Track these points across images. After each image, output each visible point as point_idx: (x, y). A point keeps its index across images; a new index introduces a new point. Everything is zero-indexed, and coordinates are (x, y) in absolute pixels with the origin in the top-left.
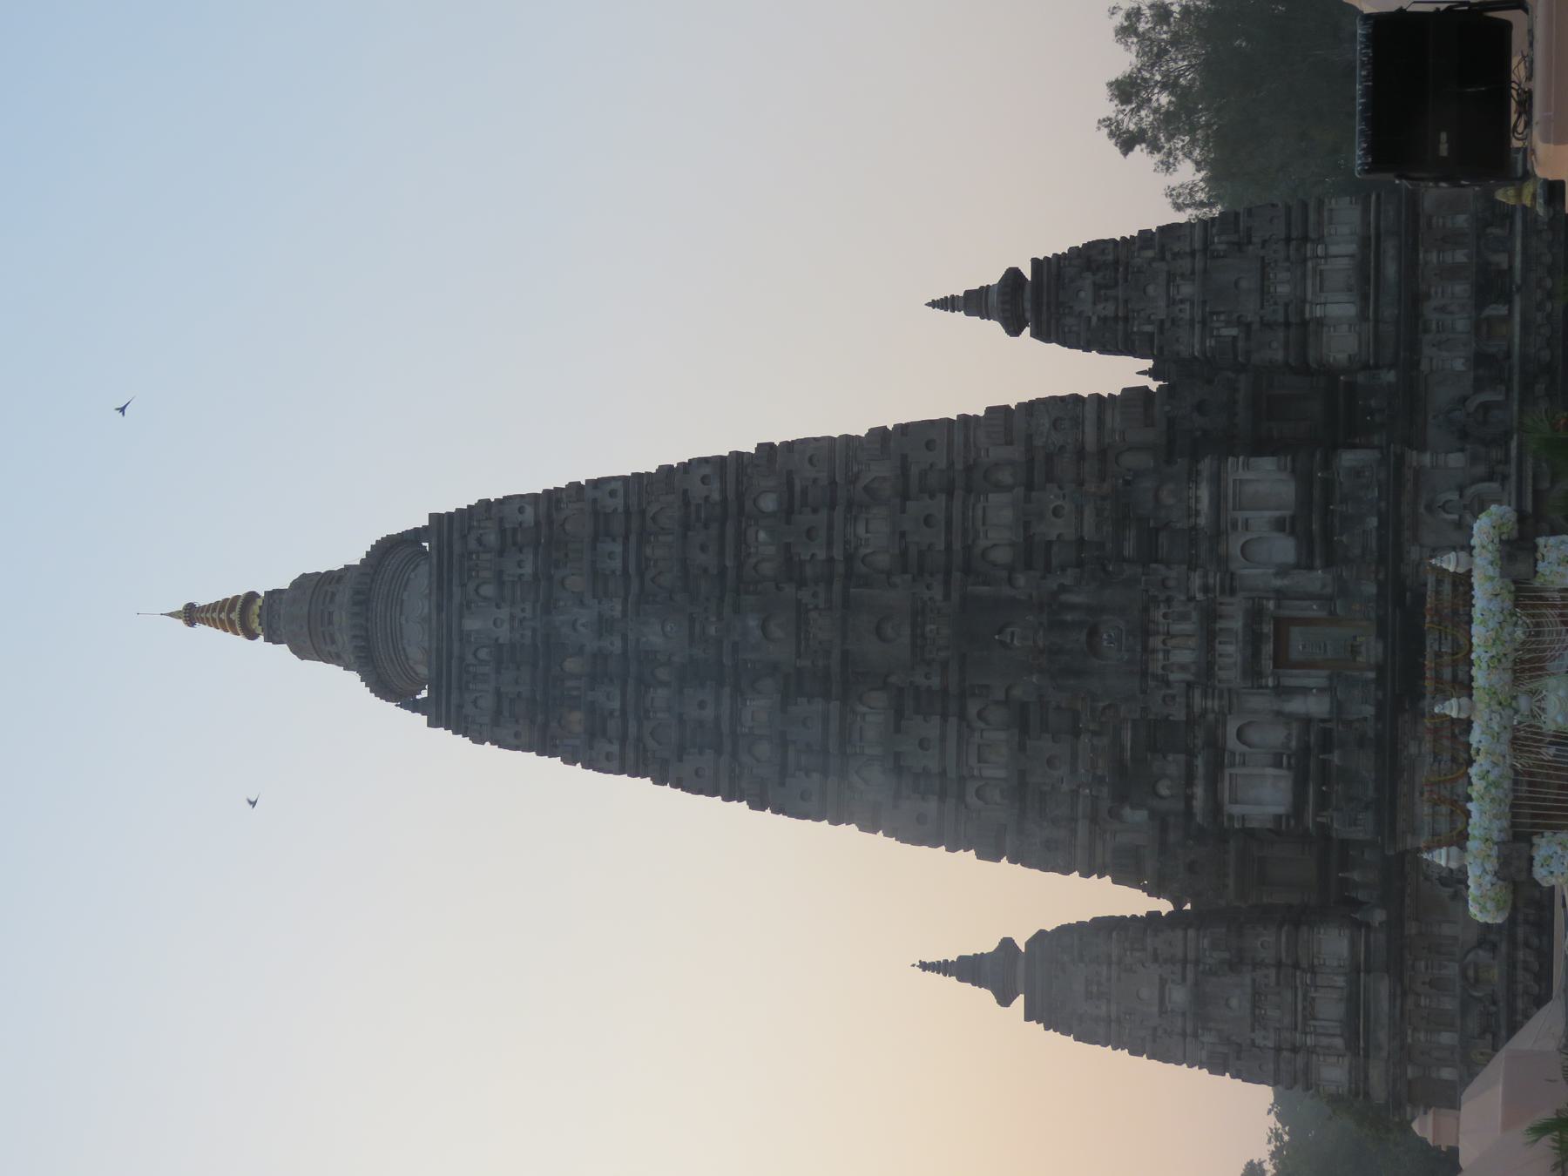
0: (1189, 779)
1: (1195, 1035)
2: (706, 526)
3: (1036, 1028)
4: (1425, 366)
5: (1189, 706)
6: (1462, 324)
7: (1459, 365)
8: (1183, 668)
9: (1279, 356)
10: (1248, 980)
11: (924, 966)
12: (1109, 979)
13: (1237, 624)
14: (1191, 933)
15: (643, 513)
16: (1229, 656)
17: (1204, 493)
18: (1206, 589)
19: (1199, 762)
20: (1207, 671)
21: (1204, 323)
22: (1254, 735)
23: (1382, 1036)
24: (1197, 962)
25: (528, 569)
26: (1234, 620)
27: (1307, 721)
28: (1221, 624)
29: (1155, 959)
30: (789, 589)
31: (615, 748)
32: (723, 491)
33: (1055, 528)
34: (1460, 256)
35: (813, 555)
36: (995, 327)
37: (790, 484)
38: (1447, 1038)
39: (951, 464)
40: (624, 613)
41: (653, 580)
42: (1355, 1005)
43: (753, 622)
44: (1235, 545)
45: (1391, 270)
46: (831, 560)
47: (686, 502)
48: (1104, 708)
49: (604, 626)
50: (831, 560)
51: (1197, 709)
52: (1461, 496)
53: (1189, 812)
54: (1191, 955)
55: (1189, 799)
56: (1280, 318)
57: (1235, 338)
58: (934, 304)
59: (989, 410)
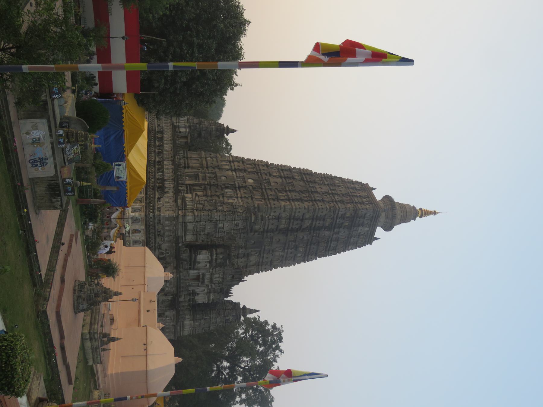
0: (216, 259)
1: (217, 220)
13: (206, 280)
15: (326, 251)
17: (211, 298)
20: (212, 274)
23: (180, 227)
25: (352, 239)
26: (207, 282)
27: (194, 269)
33: (243, 260)
38: (167, 228)
42: (185, 230)
43: (305, 238)
44: (206, 291)
45: (178, 328)
46: (288, 249)
49: (338, 233)
55: (216, 256)
58: (259, 311)
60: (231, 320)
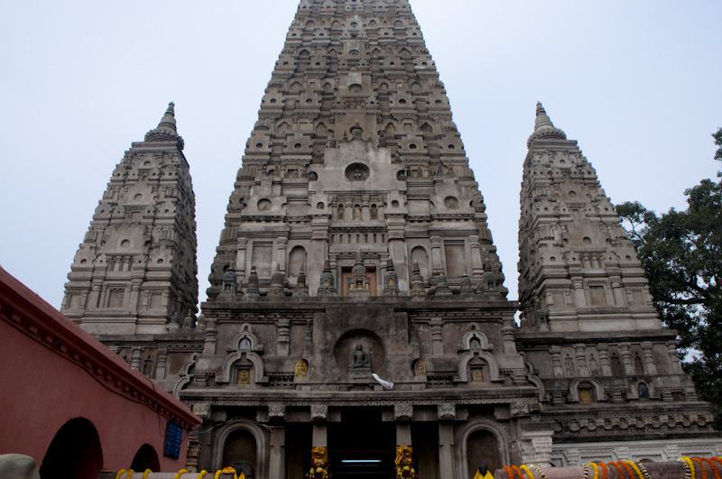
0: (268, 219)
1: (109, 225)
2: (403, 64)
3: (128, 147)
4: (555, 348)
5: (317, 216)
6: (585, 373)
7: (558, 371)
8: (341, 216)
9: (547, 262)
10: (138, 251)
11: (172, 105)
12: (149, 180)
14: (173, 221)
16: (349, 241)
18: (391, 224)
19: (281, 224)
21: (559, 223)
22: (298, 256)
24: (153, 225)
28: (371, 235)
29: (157, 204)
30: (376, 94)
31: (298, 36)
32: (420, 70)
34: (630, 370)
35: (391, 102)
36: (531, 131)
37: (427, 94)
39: (441, 155)
40: (360, 39)
41: (376, 49)
43: (359, 80)
47: (412, 59)
48: (315, 173)
50: (391, 109)
51: (315, 221)
52: (484, 350)
53: (249, 219)
54: (157, 221)
56: (571, 262)
57: (553, 238)
59: (472, 171)
60: (567, 165)
